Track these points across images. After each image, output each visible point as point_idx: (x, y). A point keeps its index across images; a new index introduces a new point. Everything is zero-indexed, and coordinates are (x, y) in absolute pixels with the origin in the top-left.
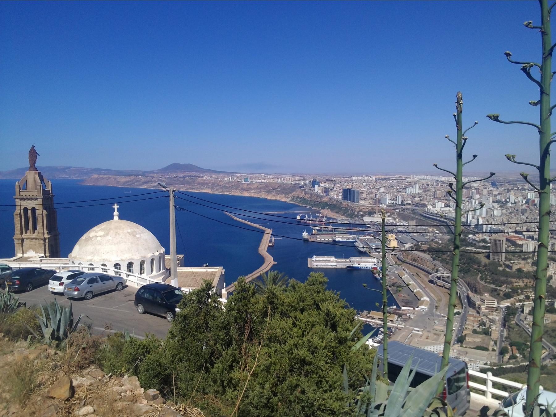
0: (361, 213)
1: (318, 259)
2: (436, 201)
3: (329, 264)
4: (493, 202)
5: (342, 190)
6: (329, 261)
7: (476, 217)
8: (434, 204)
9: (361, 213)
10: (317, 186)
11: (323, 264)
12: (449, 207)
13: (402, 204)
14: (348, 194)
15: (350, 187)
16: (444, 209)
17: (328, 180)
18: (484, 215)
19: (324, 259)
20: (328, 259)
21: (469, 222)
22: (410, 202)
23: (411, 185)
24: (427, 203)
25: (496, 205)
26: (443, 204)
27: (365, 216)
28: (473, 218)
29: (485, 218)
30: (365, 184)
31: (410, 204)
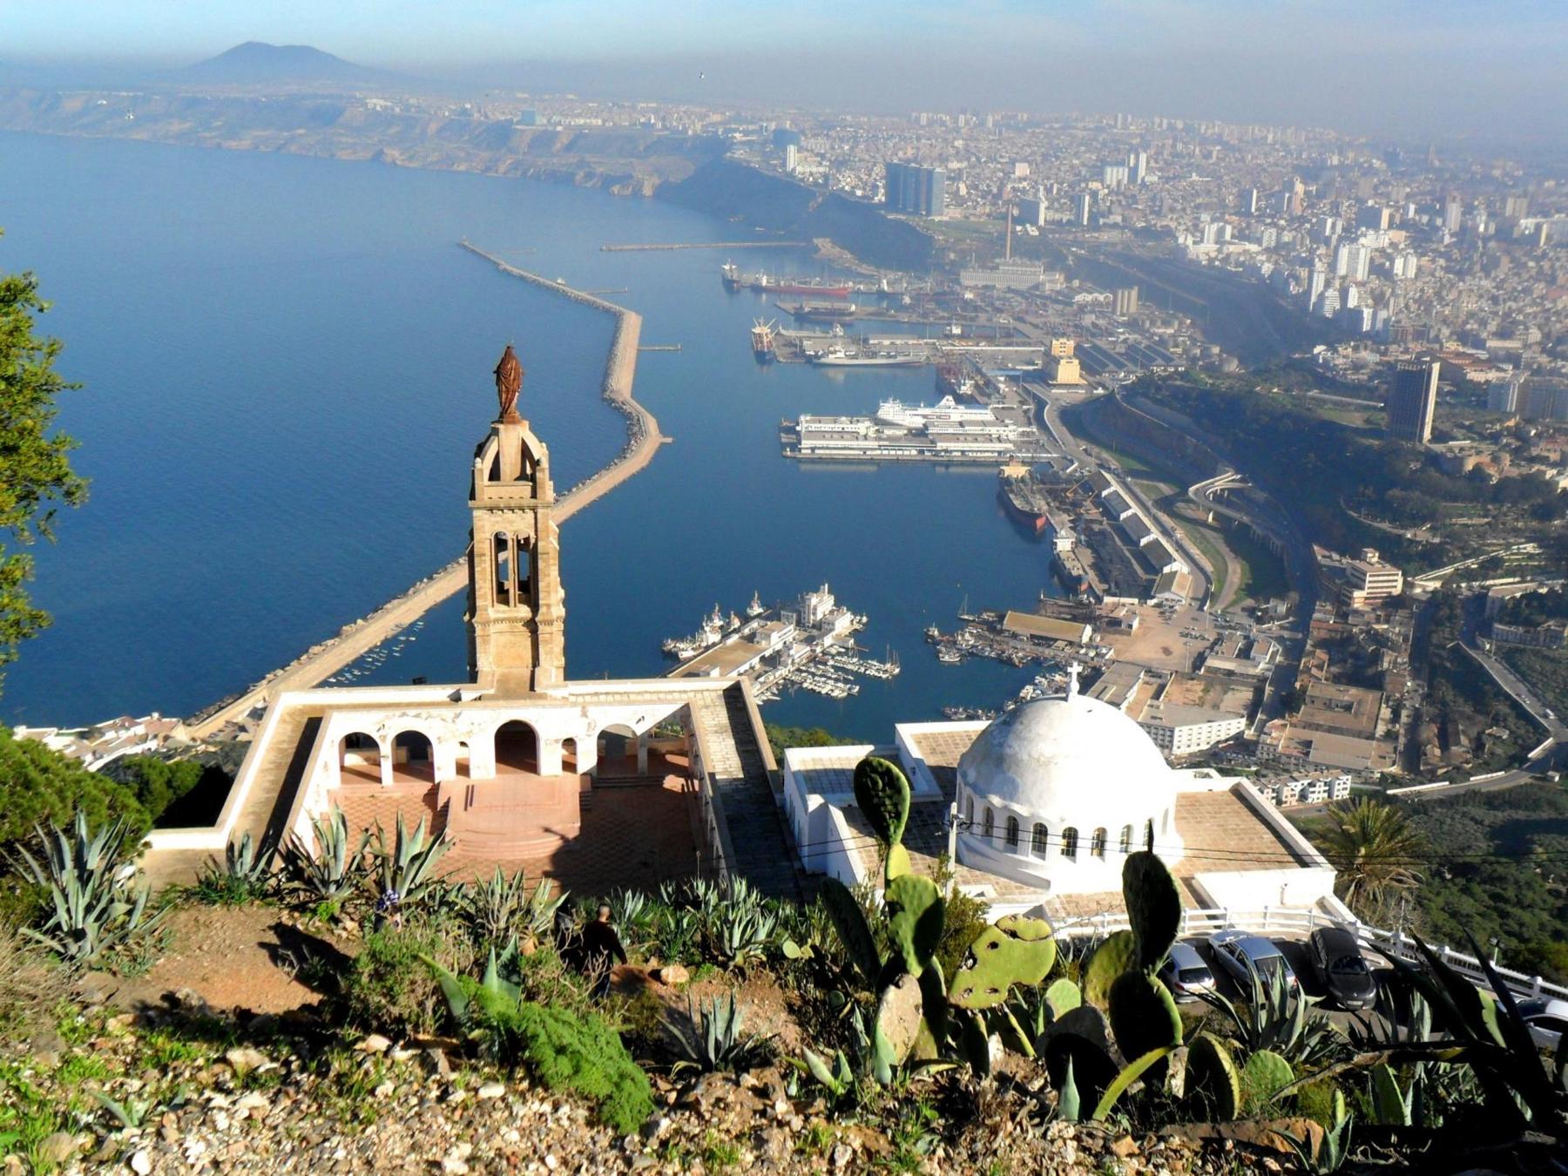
0: (952, 256)
1: (814, 427)
2: (1205, 217)
3: (854, 444)
4: (1391, 226)
5: (879, 170)
6: (855, 436)
7: (1337, 283)
8: (1196, 229)
9: (952, 256)
10: (792, 149)
11: (832, 443)
12: (1249, 239)
13: (1094, 225)
14: (908, 185)
15: (910, 152)
16: (1232, 248)
17: (825, 128)
18: (1361, 273)
19: (838, 427)
20: (850, 427)
21: (1313, 299)
22: (1119, 219)
23: (1117, 152)
24: (1173, 225)
25: (1400, 236)
26: (1229, 229)
27: (965, 267)
28: (1328, 284)
29: (1362, 284)
30: (959, 143)
31: (1115, 226)
